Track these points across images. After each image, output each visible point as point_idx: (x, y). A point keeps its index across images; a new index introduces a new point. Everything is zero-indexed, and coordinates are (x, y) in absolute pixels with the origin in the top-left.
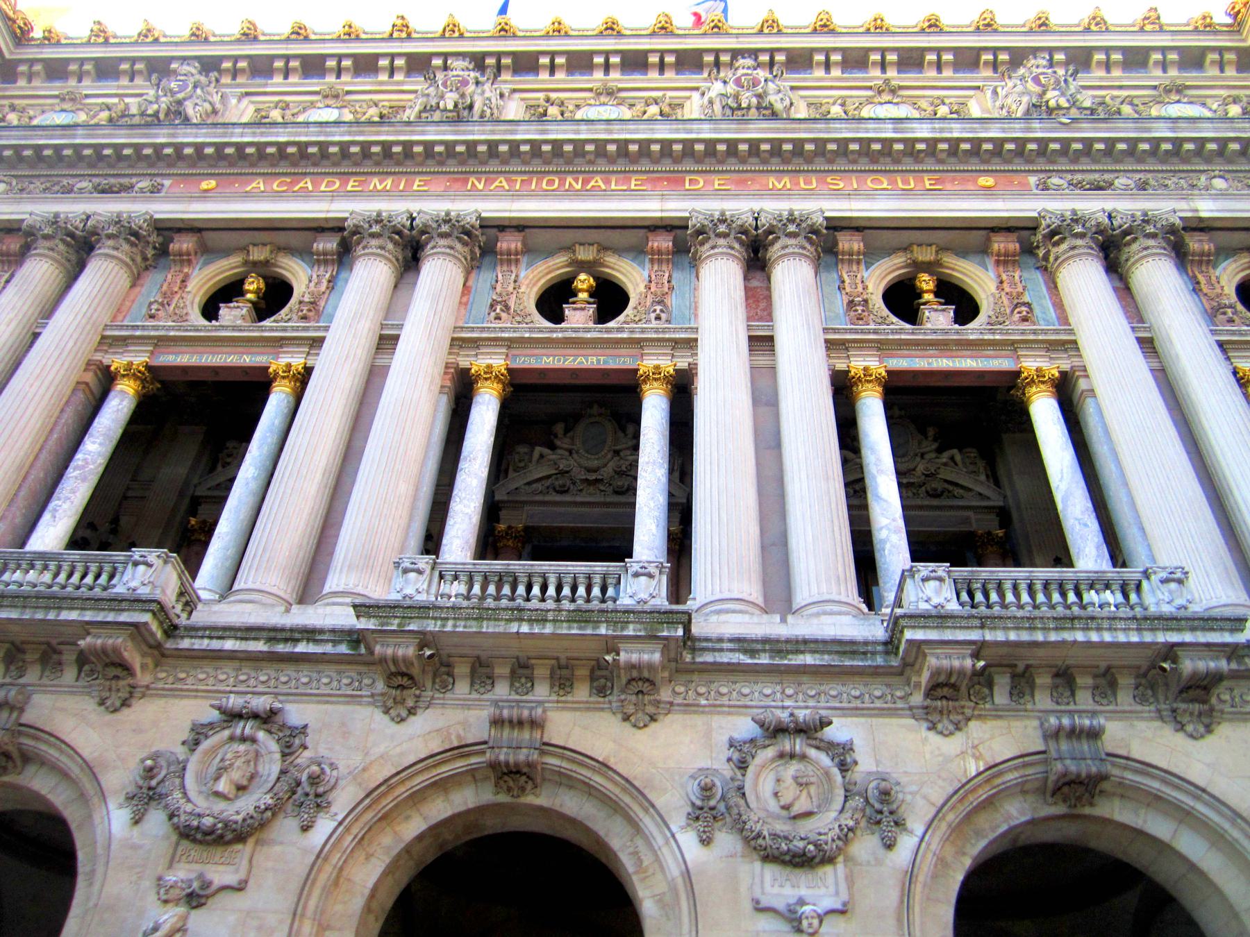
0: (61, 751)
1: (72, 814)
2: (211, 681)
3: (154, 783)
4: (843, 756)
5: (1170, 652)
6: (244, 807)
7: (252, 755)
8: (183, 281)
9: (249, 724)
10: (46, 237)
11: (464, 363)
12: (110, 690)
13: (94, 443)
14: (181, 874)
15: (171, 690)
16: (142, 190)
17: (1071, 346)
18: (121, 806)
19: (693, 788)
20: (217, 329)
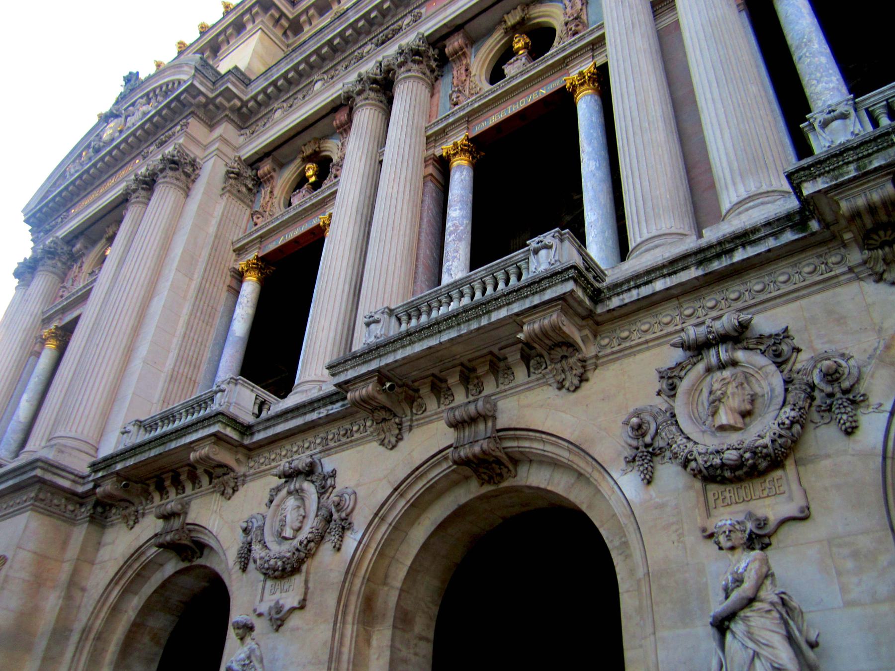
0: (544, 442)
1: (579, 497)
2: (657, 328)
3: (648, 439)
6: (763, 430)
7: (741, 378)
8: (467, 70)
9: (722, 349)
10: (360, 93)
12: (563, 371)
13: (455, 210)
14: (725, 518)
15: (620, 351)
16: (408, 25)
18: (625, 472)
20: (509, 82)
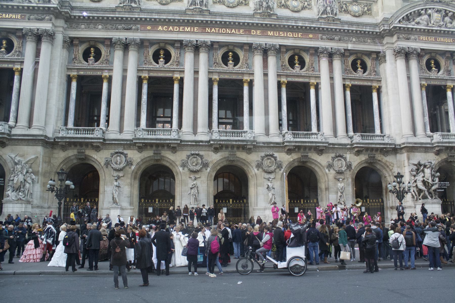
4: (275, 158)
5: (319, 146)
11: (211, 77)
17: (319, 77)
19: (256, 163)
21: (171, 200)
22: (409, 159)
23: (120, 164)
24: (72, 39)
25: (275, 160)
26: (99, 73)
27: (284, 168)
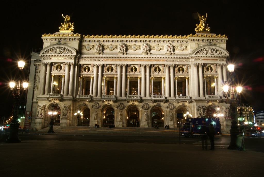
19: (141, 107)
21: (113, 119)
22: (196, 105)
23: (97, 106)
24: (80, 64)
25: (148, 105)
26: (89, 76)
27: (151, 108)
